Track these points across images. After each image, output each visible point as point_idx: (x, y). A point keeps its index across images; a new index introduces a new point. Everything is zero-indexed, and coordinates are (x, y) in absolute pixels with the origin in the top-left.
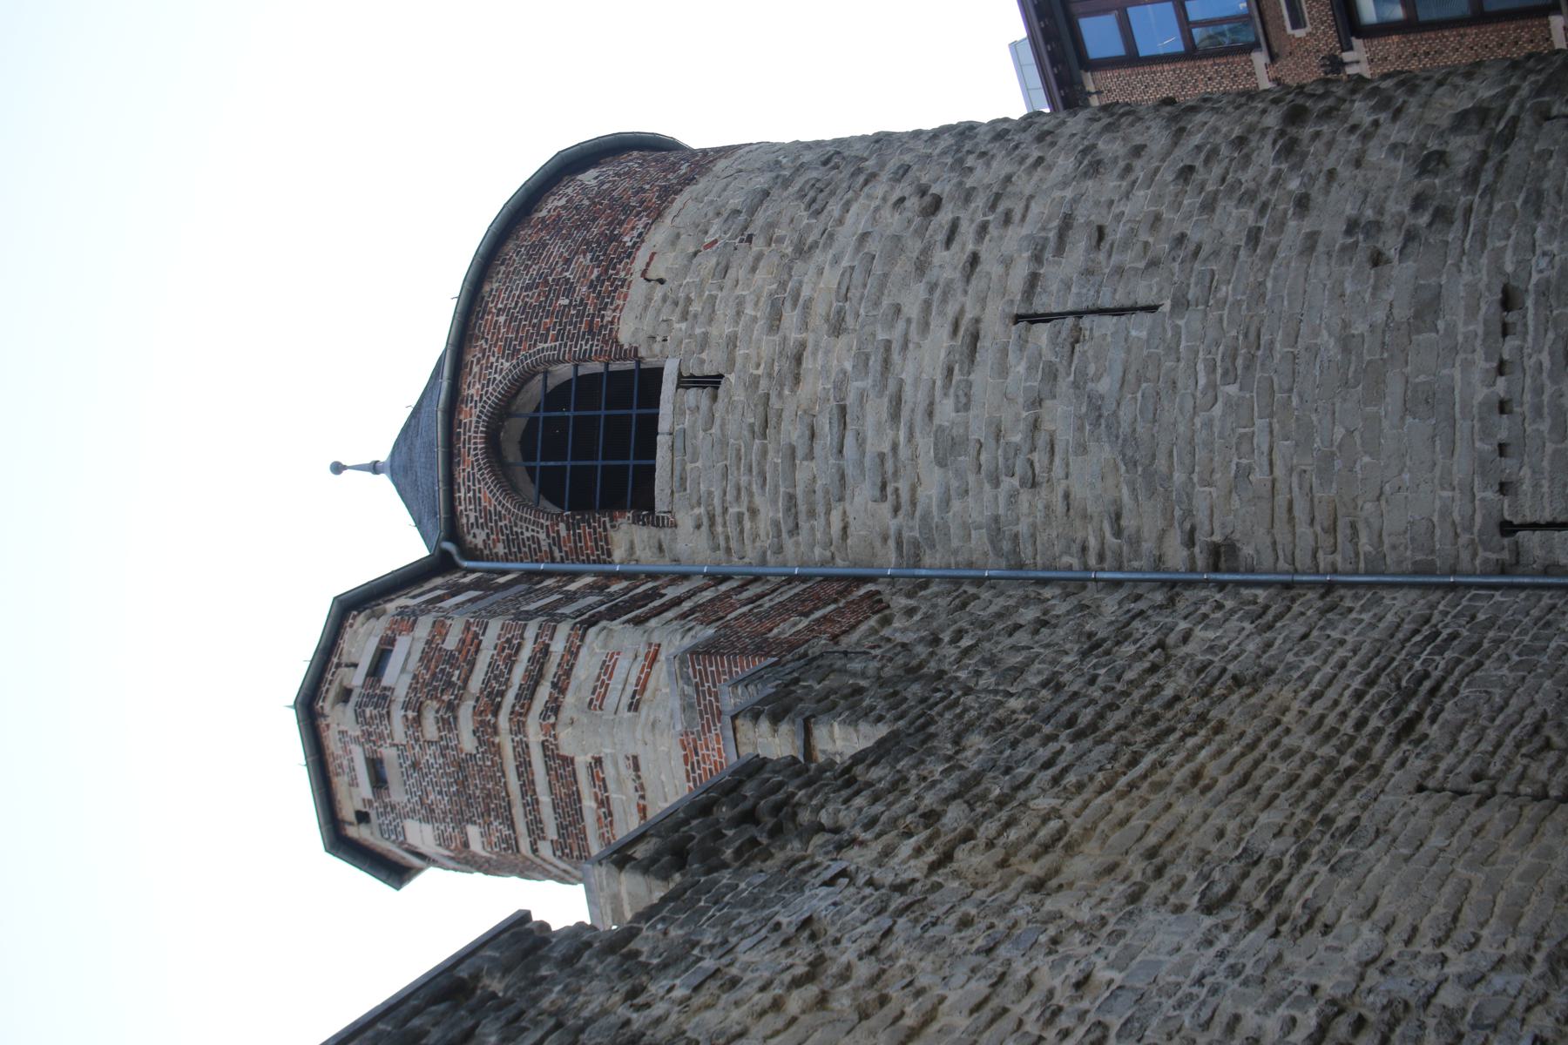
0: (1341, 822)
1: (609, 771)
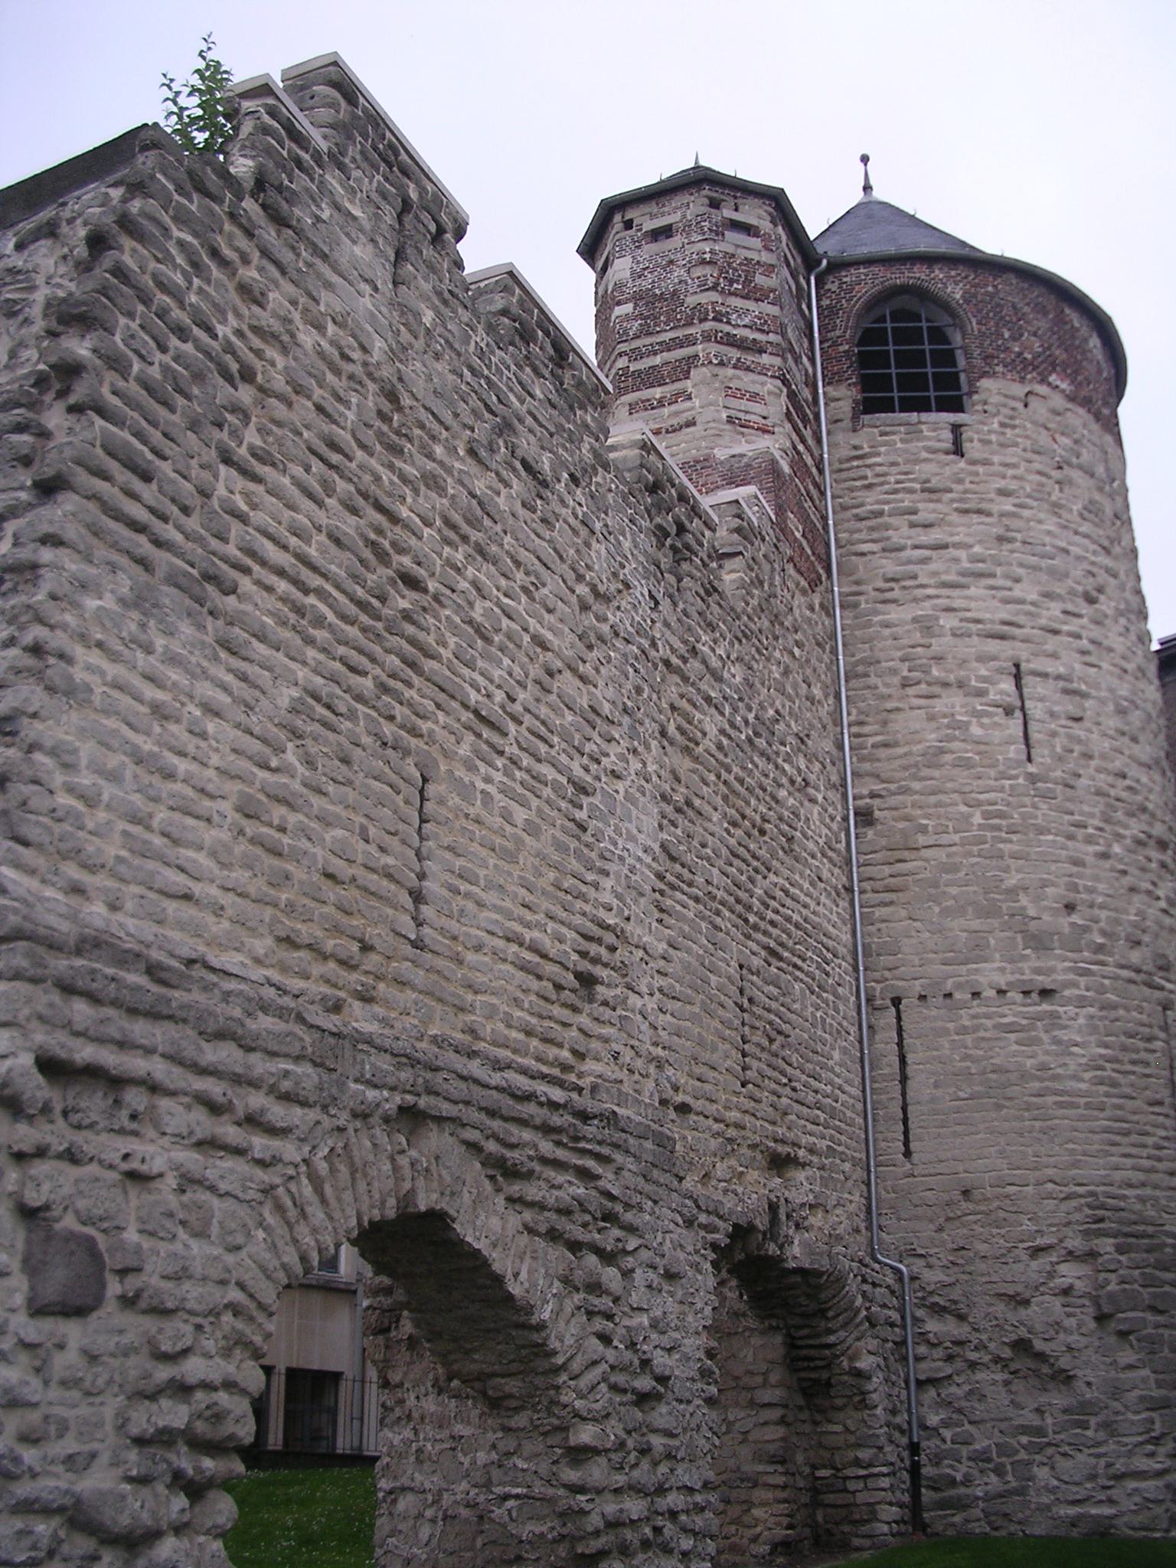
0: (718, 920)
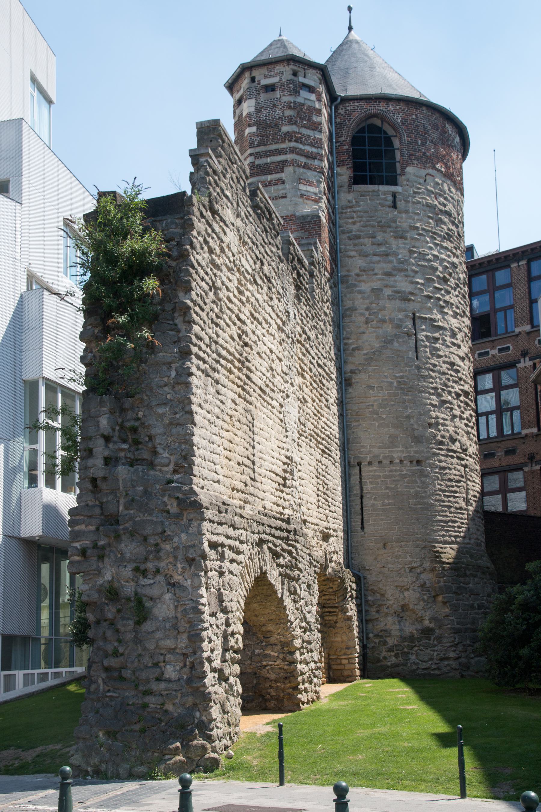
1: (281, 187)
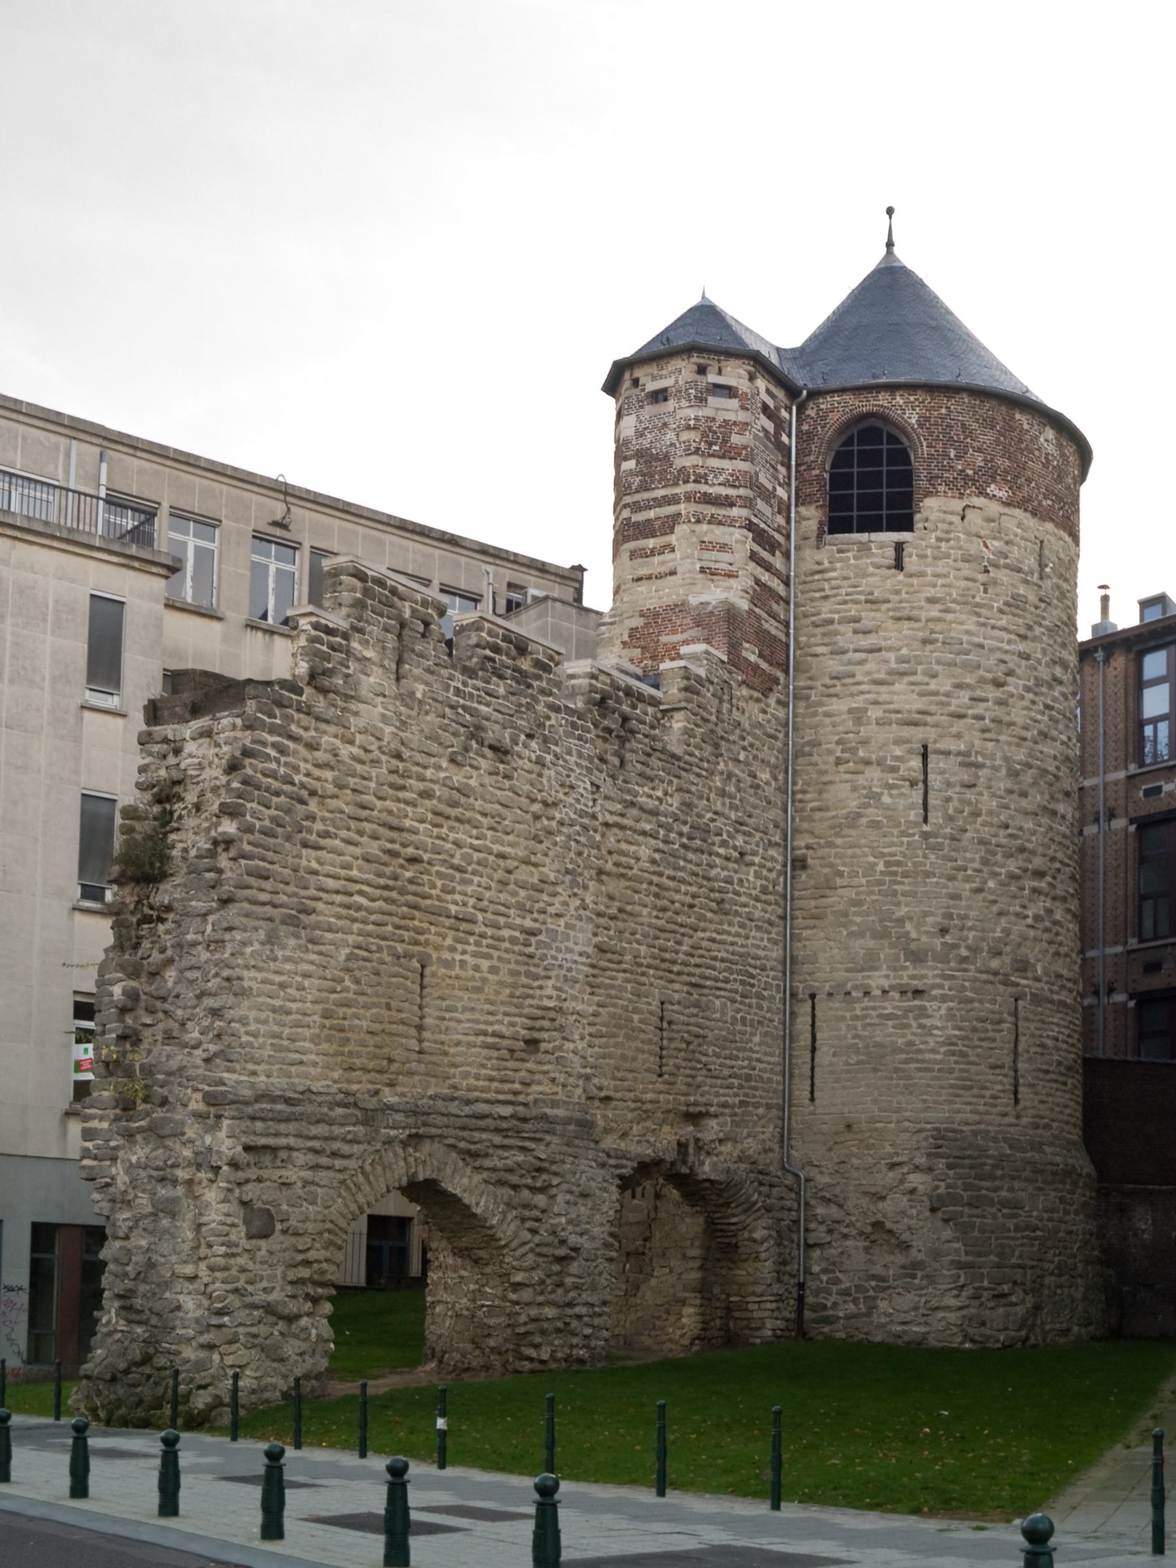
0: (644, 979)
